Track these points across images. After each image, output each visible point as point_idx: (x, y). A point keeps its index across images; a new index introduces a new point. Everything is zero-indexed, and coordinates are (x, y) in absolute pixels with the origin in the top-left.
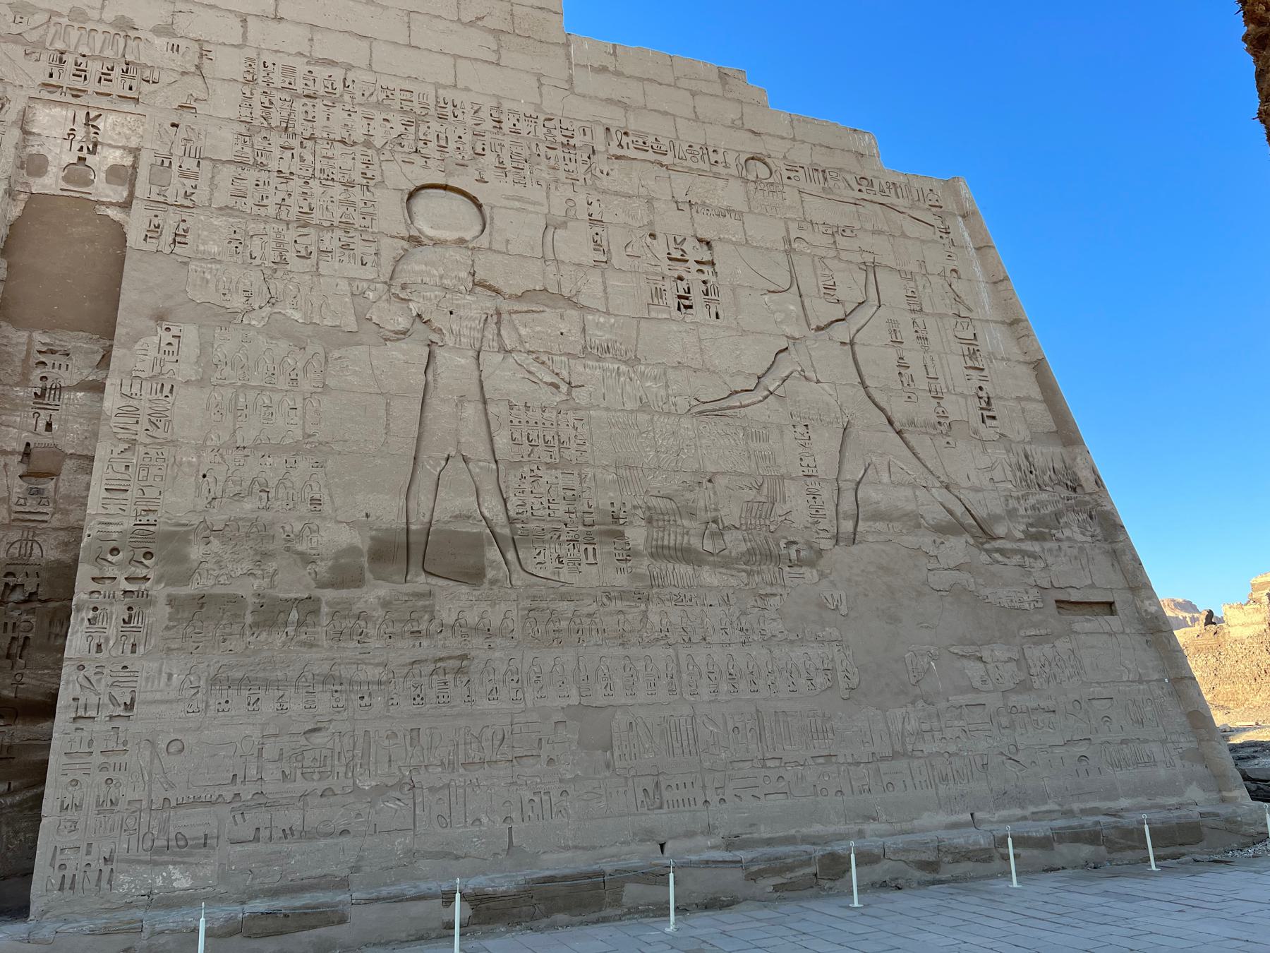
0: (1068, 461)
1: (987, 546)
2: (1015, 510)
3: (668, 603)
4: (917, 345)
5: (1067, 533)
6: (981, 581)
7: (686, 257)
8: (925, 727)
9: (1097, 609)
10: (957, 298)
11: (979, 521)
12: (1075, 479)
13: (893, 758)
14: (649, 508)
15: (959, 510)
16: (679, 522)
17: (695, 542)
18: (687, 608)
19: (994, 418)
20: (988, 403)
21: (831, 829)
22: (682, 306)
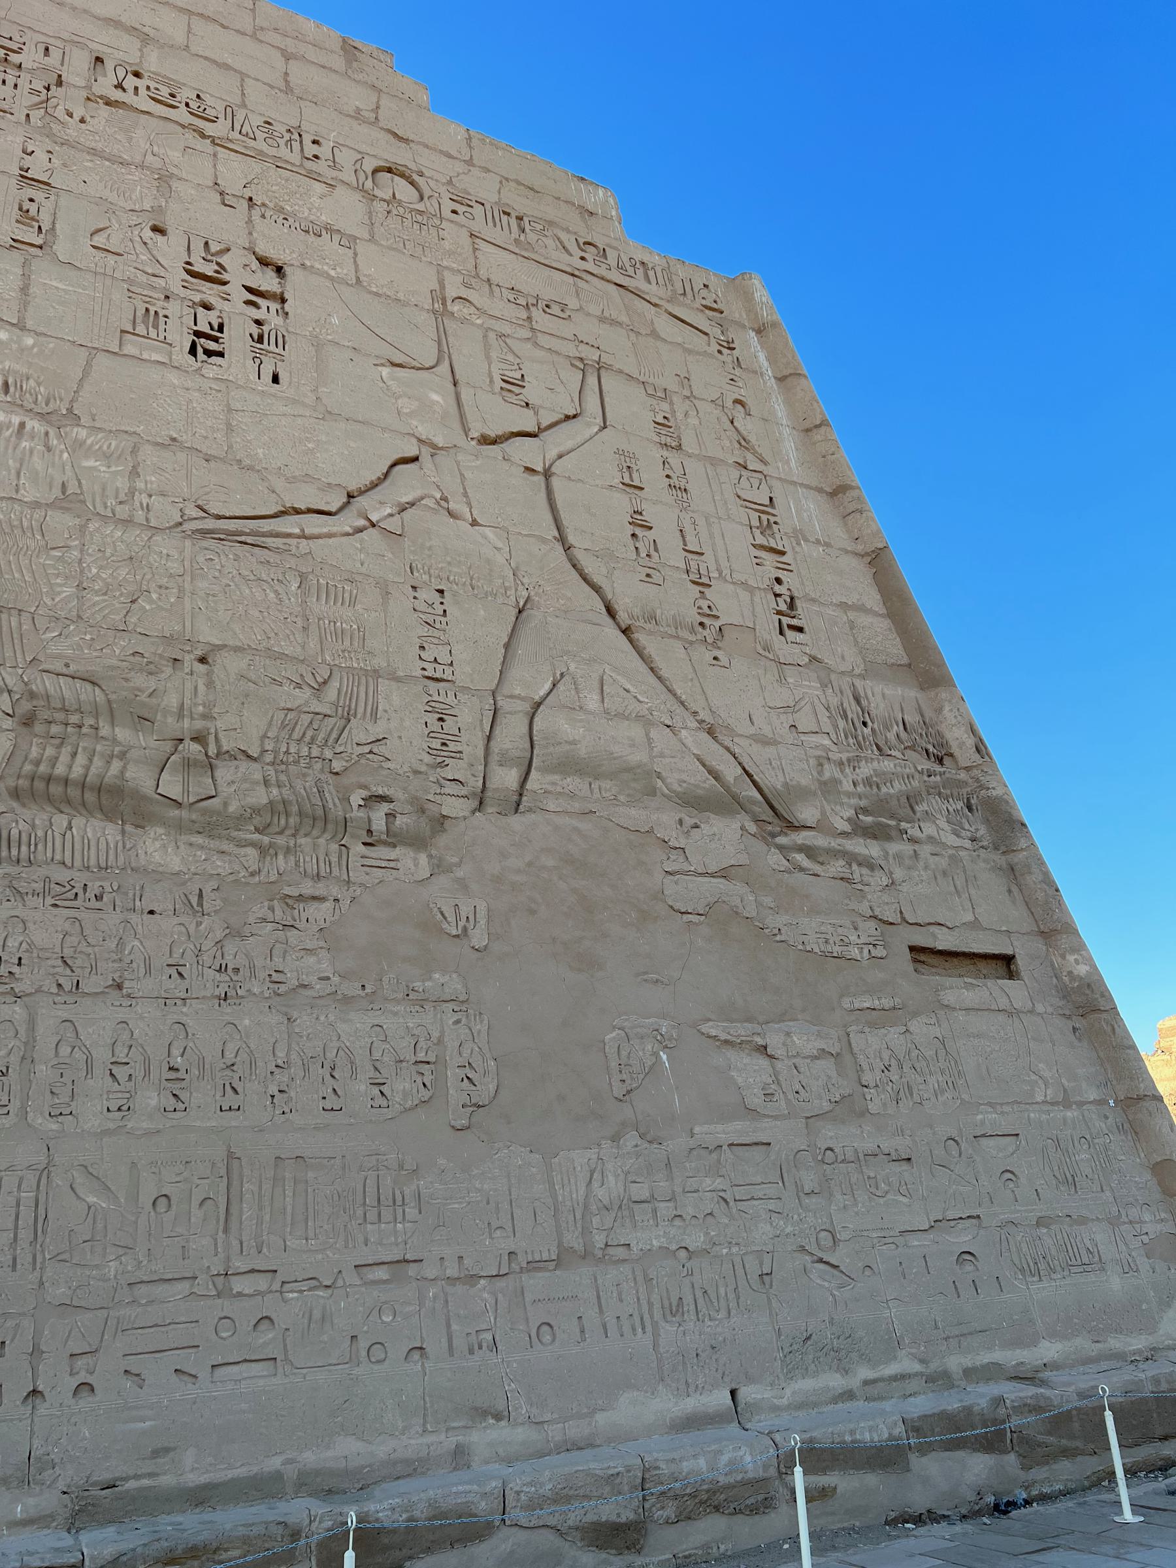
0: (929, 714)
1: (782, 840)
2: (836, 782)
3: (31, 901)
4: (668, 497)
5: (929, 829)
6: (768, 901)
7: (225, 277)
8: (640, 1191)
9: (982, 965)
10: (743, 443)
11: (770, 796)
12: (942, 744)
13: (559, 1263)
14: (32, 695)
15: (731, 772)
16: (105, 731)
17: (140, 777)
18: (82, 915)
19: (800, 630)
20: (792, 605)
21: (382, 1449)
22: (200, 350)
